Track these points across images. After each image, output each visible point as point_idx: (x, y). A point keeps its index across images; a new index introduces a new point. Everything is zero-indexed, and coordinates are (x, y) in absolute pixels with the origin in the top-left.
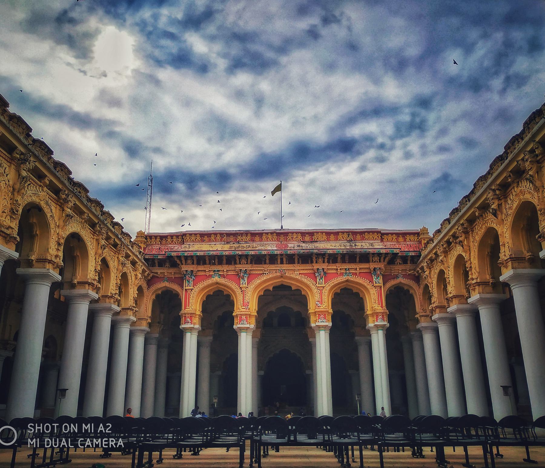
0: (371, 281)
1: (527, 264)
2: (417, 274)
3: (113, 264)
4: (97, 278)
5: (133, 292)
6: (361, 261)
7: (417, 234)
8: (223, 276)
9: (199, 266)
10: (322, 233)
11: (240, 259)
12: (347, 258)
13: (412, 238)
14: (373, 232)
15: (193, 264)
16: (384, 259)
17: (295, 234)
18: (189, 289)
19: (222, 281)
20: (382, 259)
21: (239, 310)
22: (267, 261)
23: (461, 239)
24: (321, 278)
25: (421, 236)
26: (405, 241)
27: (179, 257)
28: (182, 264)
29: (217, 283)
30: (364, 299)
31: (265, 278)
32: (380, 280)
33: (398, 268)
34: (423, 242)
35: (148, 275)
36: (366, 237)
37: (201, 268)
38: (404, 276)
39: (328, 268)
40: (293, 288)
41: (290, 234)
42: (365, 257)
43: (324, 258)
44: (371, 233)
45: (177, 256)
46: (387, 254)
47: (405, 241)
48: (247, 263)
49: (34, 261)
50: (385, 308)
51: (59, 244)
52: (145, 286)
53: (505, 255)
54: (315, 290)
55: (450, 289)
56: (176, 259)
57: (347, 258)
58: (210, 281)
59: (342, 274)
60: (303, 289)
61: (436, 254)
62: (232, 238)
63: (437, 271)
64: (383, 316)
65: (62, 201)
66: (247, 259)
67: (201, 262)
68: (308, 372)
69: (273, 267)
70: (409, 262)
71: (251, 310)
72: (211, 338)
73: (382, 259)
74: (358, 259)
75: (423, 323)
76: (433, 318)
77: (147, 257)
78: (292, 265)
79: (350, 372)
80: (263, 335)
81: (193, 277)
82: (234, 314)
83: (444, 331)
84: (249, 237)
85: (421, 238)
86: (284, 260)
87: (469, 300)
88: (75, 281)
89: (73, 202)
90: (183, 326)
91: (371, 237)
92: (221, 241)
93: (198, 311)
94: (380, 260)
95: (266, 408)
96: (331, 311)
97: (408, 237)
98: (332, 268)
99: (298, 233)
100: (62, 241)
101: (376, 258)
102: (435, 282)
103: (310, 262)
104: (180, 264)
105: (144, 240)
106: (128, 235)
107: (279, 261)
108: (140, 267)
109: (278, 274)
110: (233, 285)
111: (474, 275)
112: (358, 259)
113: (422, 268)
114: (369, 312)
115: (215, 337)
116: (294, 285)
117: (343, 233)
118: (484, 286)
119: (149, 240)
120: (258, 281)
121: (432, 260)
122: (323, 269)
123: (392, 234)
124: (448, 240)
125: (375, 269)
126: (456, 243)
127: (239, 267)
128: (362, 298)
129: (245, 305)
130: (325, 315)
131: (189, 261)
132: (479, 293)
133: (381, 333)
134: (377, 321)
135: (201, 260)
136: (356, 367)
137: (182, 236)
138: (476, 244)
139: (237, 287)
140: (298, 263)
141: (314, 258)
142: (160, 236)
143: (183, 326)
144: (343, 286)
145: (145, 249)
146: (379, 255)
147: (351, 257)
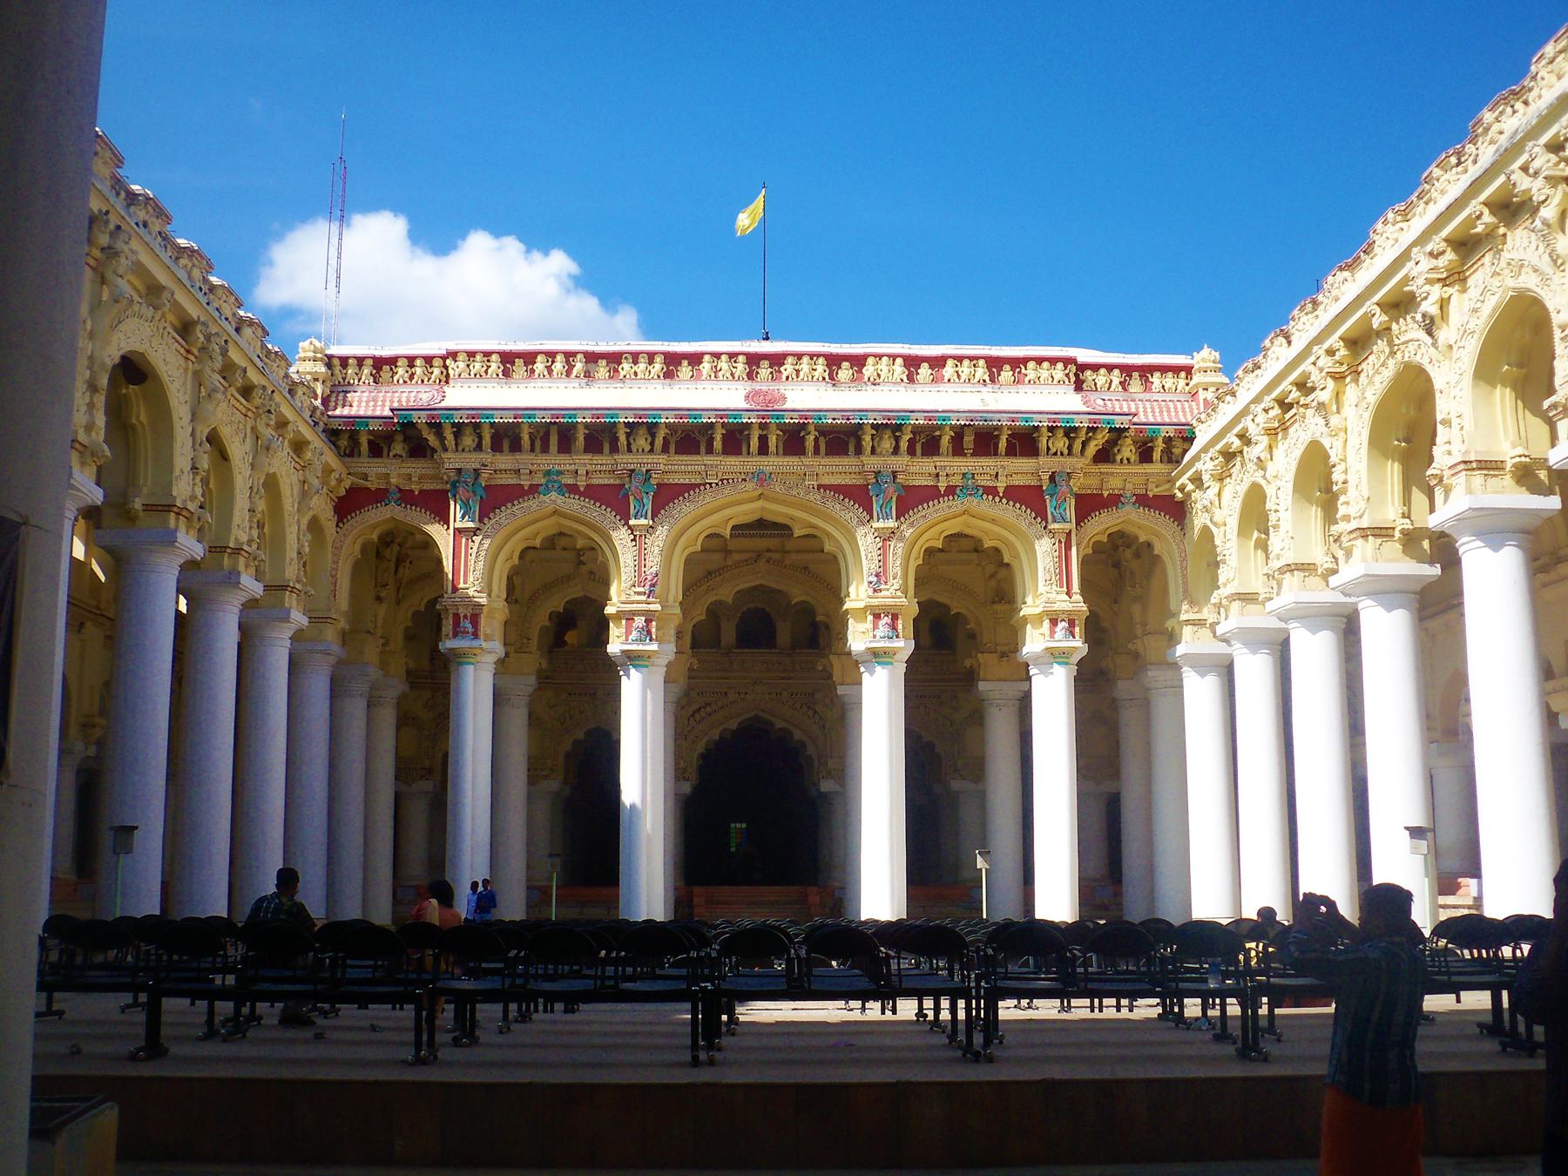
0: (1041, 513)
1: (1508, 480)
2: (1179, 495)
3: (238, 450)
4: (199, 491)
5: (294, 536)
6: (1011, 452)
7: (1188, 370)
8: (573, 489)
9: (498, 456)
11: (628, 435)
12: (969, 440)
13: (1169, 380)
14: (1053, 361)
15: (479, 448)
16: (1084, 444)
19: (574, 504)
20: (1077, 446)
21: (620, 595)
22: (718, 444)
23: (1324, 396)
24: (888, 501)
25: (1197, 378)
27: (436, 427)
28: (445, 450)
30: (1015, 564)
32: (1070, 511)
33: (1125, 475)
35: (340, 481)
37: (505, 461)
38: (1143, 500)
40: (797, 532)
41: (790, 359)
42: (1024, 440)
43: (897, 439)
44: (1046, 365)
45: (429, 425)
48: (651, 451)
50: (1077, 597)
51: (93, 387)
53: (1449, 453)
55: (1275, 542)
57: (969, 440)
58: (532, 504)
59: (951, 491)
60: (828, 534)
61: (1244, 437)
62: (602, 369)
63: (1242, 489)
64: (1072, 623)
65: (96, 253)
66: (653, 436)
67: (506, 446)
68: (826, 786)
69: (732, 461)
70: (1157, 455)
72: (532, 680)
73: (1077, 446)
74: (1003, 444)
75: (1190, 643)
76: (1220, 630)
77: (335, 425)
79: (956, 785)
80: (692, 674)
81: (480, 492)
82: (609, 610)
83: (1253, 672)
85: (1196, 385)
86: (772, 440)
87: (1334, 581)
88: (138, 504)
90: (448, 644)
94: (1070, 448)
95: (697, 890)
97: (1156, 379)
98: (920, 470)
99: (819, 355)
100: (104, 381)
101: (1061, 443)
102: (1233, 523)
103: (851, 448)
104: (439, 449)
105: (323, 369)
107: (754, 443)
108: (321, 452)
111: (1352, 505)
112: (1003, 444)
113: (1197, 480)
115: (545, 680)
116: (801, 519)
118: (1379, 541)
119: (338, 369)
120: (684, 510)
121: (1229, 456)
122: (894, 473)
123: (1110, 368)
125: (1052, 478)
126: (1306, 406)
127: (625, 460)
128: (1008, 565)
130: (895, 617)
131: (468, 440)
132: (1364, 560)
135: (506, 434)
136: (977, 770)
137: (444, 358)
138: (1367, 416)
140: (817, 452)
141: (868, 438)
142: (374, 358)
143: (448, 644)
144: (953, 527)
145: (325, 401)
146: (1070, 432)
147: (981, 438)
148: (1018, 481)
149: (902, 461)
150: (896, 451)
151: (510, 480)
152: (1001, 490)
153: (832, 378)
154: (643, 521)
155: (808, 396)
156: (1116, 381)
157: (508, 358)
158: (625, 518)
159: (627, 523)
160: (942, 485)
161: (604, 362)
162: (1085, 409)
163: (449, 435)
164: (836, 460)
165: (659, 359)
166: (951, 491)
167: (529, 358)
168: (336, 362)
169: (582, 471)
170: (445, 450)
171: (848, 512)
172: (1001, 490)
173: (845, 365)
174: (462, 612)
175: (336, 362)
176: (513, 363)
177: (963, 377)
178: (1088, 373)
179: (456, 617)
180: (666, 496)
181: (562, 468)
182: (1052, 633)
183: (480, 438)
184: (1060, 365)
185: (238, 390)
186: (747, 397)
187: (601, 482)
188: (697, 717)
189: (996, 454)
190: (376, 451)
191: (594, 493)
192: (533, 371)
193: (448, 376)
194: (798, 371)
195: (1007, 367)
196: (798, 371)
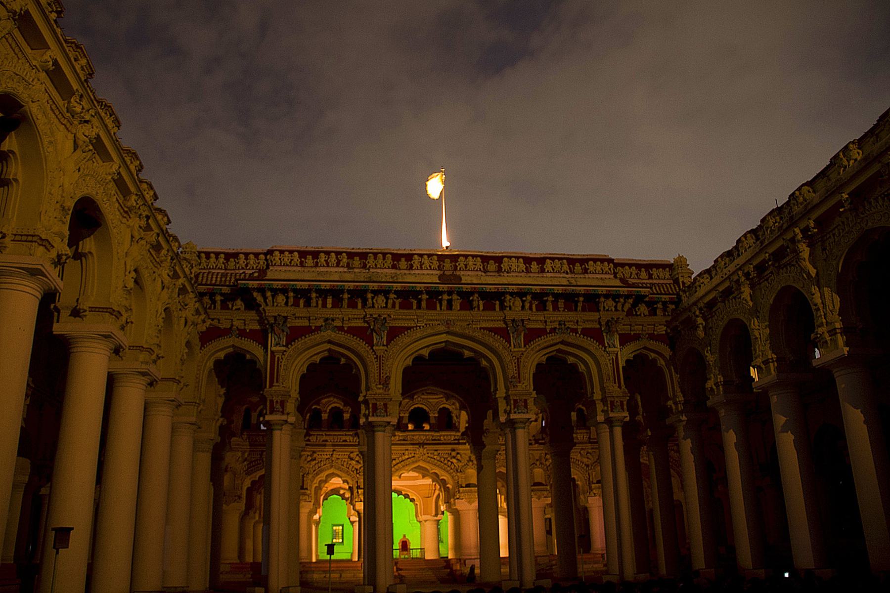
0: (601, 342)
6: (584, 310)
8: (341, 329)
10: (518, 258)
12: (561, 303)
17: (470, 258)
18: (278, 351)
19: (341, 337)
22: (424, 304)
24: (519, 335)
26: (650, 277)
27: (262, 290)
31: (419, 335)
34: (681, 280)
35: (204, 321)
36: (591, 269)
37: (301, 311)
38: (652, 337)
41: (461, 258)
42: (592, 300)
44: (599, 263)
46: (627, 297)
47: (650, 277)
48: (386, 307)
49: (7, 240)
52: (196, 342)
54: (507, 358)
56: (255, 294)
58: (317, 337)
60: (485, 357)
62: (357, 261)
64: (622, 403)
67: (302, 302)
70: (658, 312)
71: (392, 391)
77: (202, 288)
78: (468, 312)
81: (286, 330)
82: (361, 399)
89: (96, 130)
91: (599, 268)
92: (338, 265)
93: (293, 391)
96: (534, 394)
97: (654, 271)
99: (476, 256)
101: (610, 303)
106: (176, 239)
107: (445, 303)
109: (442, 328)
114: (598, 396)
117: (553, 259)
120: (403, 340)
121: (711, 304)
122: (523, 321)
123: (630, 265)
124: (764, 261)
130: (525, 401)
133: (618, 431)
134: (612, 411)
135: (303, 295)
137: (266, 254)
146: (615, 297)
148: (588, 326)
150: (523, 307)
151: (306, 323)
155: (471, 278)
156: (634, 273)
157: (303, 254)
158: (372, 346)
159: (372, 348)
161: (358, 258)
162: (621, 285)
163: (269, 294)
165: (389, 256)
166: (553, 330)
167: (315, 254)
170: (267, 305)
171: (497, 342)
173: (491, 262)
175: (203, 255)
179: (272, 401)
180: (394, 333)
182: (612, 411)
183: (287, 298)
185: (153, 247)
186: (440, 277)
187: (356, 325)
189: (576, 310)
190: (224, 306)
192: (317, 263)
194: (466, 266)
195: (578, 264)
196: (466, 266)
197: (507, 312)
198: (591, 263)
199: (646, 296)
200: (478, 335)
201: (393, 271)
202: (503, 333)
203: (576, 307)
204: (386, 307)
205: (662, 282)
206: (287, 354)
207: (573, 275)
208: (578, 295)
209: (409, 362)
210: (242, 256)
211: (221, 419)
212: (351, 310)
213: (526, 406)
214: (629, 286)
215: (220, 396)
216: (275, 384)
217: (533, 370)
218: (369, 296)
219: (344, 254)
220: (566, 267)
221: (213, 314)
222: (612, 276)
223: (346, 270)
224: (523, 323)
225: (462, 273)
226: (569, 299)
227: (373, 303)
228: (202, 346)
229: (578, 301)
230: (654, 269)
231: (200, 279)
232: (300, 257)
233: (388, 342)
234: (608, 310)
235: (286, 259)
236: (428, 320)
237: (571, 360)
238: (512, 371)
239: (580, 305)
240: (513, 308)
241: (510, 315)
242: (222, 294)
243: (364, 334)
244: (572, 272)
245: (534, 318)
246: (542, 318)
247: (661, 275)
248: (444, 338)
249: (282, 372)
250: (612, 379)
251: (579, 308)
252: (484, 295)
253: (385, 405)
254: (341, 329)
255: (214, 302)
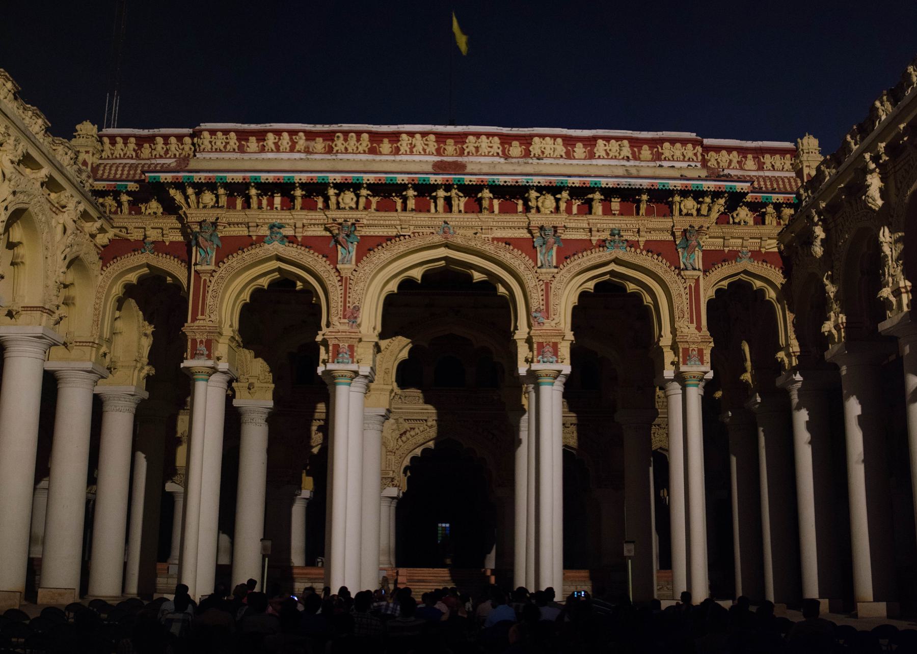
6: (649, 213)
8: (292, 240)
13: (777, 160)
17: (484, 138)
18: (205, 272)
19: (291, 252)
26: (761, 167)
27: (180, 186)
29: (279, 258)
37: (238, 215)
38: (756, 255)
39: (568, 225)
41: (471, 138)
44: (678, 145)
46: (716, 195)
52: (92, 257)
56: (172, 192)
59: (602, 244)
69: (422, 218)
70: (768, 219)
81: (216, 241)
84: (364, 144)
86: (455, 203)
91: (678, 154)
92: (292, 149)
95: (402, 571)
96: (570, 336)
97: (767, 159)
98: (575, 227)
101: (690, 204)
107: (441, 202)
109: (437, 239)
110: (320, 265)
114: (666, 340)
120: (381, 255)
122: (555, 228)
129: (352, 315)
130: (555, 346)
134: (685, 363)
137: (192, 136)
139: (330, 268)
148: (655, 237)
149: (560, 219)
150: (557, 209)
151: (242, 231)
152: (642, 244)
153: (503, 151)
154: (347, 266)
156: (735, 160)
160: (595, 239)
163: (190, 191)
164: (508, 217)
166: (602, 244)
168: (106, 140)
169: (299, 224)
170: (189, 207)
171: (517, 260)
172: (642, 244)
173: (515, 143)
174: (198, 337)
176: (247, 140)
177: (611, 154)
178: (712, 154)
179: (194, 341)
180: (368, 246)
181: (283, 221)
183: (217, 196)
184: (690, 146)
188: (404, 438)
191: (309, 243)
193: (195, 150)
194: (477, 148)
195: (645, 147)
196: (477, 148)
197: (533, 215)
198: (667, 145)
199: (745, 194)
200: (489, 249)
201: (370, 157)
202: (527, 247)
203: (638, 209)
204: (357, 208)
205: (777, 174)
206: (216, 275)
207: (637, 163)
208: (640, 191)
209: (393, 287)
210: (160, 140)
211: (147, 368)
212: (304, 212)
213: (555, 352)
214: (718, 178)
215: (146, 335)
216: (200, 317)
217: (574, 299)
218: (332, 192)
219: (301, 134)
220: (626, 151)
221: (119, 220)
222: (699, 165)
223: (303, 156)
224: (556, 232)
225: (471, 159)
226: (628, 197)
227: (338, 203)
228: (105, 265)
229: (639, 201)
230: (767, 156)
231: (100, 172)
232: (239, 140)
233: (358, 260)
234: (687, 214)
235: (219, 143)
236: (416, 226)
237: (631, 287)
238: (536, 300)
239: (643, 206)
240: (542, 209)
241: (536, 219)
242: (129, 193)
243: (326, 246)
244: (636, 158)
245: (573, 225)
246: (585, 225)
247: (778, 165)
248: (443, 252)
249: (209, 301)
250: (687, 316)
251: (642, 211)
252: (499, 191)
253: (351, 348)
254: (292, 240)
255: (120, 204)
